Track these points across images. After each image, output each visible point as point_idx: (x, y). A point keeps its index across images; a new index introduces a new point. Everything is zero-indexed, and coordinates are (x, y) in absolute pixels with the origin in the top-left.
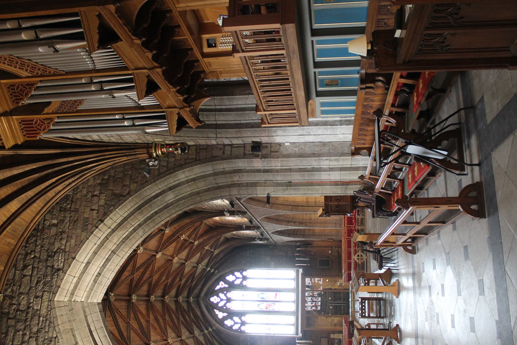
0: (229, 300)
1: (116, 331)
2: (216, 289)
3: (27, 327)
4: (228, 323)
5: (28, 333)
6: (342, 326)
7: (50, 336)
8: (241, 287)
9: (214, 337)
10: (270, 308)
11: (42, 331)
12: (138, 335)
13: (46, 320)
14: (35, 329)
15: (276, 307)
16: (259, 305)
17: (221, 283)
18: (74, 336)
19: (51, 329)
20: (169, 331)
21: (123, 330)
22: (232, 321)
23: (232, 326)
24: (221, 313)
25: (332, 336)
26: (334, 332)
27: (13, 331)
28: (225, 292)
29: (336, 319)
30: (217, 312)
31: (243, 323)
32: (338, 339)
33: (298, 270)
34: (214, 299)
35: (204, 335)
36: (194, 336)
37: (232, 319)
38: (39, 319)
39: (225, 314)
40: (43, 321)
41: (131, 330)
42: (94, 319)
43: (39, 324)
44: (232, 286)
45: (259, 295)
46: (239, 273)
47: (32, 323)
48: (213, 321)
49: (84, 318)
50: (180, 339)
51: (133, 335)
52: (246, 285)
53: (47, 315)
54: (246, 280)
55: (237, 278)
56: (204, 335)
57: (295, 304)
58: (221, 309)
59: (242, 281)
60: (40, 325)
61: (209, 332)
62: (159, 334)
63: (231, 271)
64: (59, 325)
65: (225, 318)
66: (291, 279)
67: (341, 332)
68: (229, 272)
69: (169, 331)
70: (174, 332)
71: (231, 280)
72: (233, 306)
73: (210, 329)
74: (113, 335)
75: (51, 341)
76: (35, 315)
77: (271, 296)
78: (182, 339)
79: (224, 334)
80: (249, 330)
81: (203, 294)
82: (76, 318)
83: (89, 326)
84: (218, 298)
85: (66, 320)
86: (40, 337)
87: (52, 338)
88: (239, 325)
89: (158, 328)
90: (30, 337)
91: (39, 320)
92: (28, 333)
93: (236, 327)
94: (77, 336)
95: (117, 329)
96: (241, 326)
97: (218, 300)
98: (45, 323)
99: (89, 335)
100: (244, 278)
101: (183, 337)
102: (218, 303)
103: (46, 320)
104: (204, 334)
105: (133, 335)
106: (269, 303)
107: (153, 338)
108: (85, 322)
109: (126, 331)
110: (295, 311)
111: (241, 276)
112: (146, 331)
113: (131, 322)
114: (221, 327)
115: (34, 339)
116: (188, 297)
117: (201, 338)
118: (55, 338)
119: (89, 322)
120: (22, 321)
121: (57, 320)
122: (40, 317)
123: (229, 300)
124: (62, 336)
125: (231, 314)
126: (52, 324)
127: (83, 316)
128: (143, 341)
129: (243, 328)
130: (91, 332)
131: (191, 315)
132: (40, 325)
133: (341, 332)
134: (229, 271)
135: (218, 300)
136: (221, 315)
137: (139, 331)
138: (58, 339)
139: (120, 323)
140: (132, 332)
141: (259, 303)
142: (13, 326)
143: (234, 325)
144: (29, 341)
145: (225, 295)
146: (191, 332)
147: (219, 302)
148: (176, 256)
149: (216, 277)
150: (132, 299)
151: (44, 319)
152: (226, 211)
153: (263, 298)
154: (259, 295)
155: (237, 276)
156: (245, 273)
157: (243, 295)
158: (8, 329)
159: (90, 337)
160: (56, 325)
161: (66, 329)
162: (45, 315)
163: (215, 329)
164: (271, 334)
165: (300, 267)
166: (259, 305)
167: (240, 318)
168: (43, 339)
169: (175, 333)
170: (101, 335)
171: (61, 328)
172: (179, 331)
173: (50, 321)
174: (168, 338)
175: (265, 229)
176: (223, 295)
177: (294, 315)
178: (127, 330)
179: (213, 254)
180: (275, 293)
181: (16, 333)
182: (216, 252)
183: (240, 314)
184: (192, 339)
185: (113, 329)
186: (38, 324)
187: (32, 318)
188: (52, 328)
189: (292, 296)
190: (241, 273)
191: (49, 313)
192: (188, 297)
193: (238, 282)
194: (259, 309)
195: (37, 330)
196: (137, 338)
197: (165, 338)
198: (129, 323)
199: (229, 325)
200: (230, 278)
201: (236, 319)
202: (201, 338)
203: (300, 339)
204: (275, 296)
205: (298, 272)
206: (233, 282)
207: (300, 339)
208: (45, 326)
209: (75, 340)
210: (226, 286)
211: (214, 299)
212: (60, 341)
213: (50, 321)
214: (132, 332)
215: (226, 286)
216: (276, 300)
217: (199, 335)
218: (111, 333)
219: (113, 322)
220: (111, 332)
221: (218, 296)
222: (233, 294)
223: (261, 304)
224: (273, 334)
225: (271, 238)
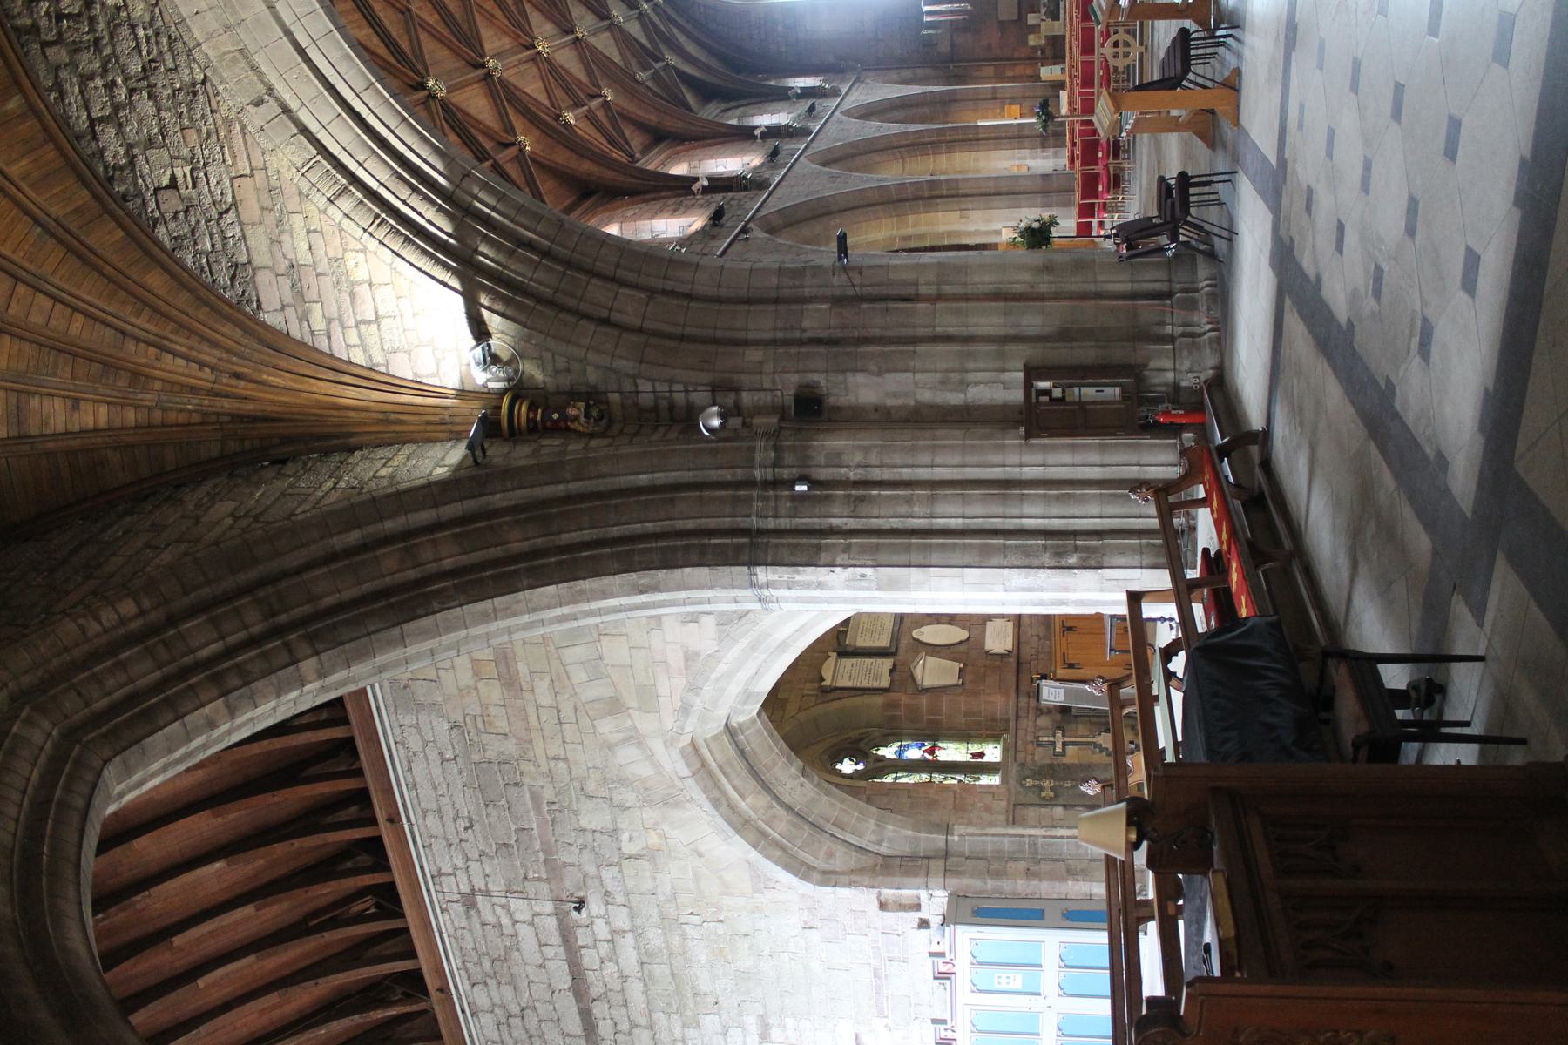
1: (376, 40)
3: (109, 61)
5: (120, 81)
7: (187, 79)
9: (670, 19)
11: (156, 68)
12: (444, 44)
13: (157, 34)
14: (135, 67)
18: (255, 69)
19: (182, 59)
20: (535, 18)
21: (394, 34)
27: (75, 80)
35: (641, 17)
36: (612, 24)
38: (136, 35)
40: (148, 39)
41: (420, 30)
42: (297, 10)
43: (140, 52)
47: (119, 49)
49: (267, 11)
50: (571, 37)
51: (428, 43)
53: (152, 19)
56: (641, 17)
60: (144, 52)
62: (504, 32)
64: (198, 45)
69: (535, 18)
70: (549, 18)
74: (367, 49)
75: (195, 94)
76: (119, 25)
78: (577, 38)
79: (702, 9)
82: (243, 17)
83: (288, 33)
85: (215, 25)
86: (160, 85)
87: (193, 85)
89: (498, 13)
90: (132, 91)
91: (136, 38)
92: (120, 81)
94: (263, 69)
95: (376, 32)
98: (157, 43)
99: (299, 60)
103: (157, 34)
104: (640, 14)
105: (428, 43)
107: (488, 46)
108: (274, 23)
109: (406, 37)
112: (465, 27)
113: (414, 10)
115: (145, 94)
117: (634, 29)
118: (203, 82)
119: (288, 24)
120: (88, 48)
121: (188, 29)
122: (133, 27)
124: (221, 76)
126: (180, 44)
127: (264, 7)
128: (464, 59)
130: (301, 52)
132: (144, 52)
137: (445, 32)
138: (213, 85)
139: (381, 15)
140: (423, 36)
142: (66, 65)
144: (131, 102)
146: (602, 14)
151: (150, 32)
158: (57, 76)
159: (303, 65)
160: (192, 45)
161: (224, 54)
162: (147, 18)
168: (170, 91)
169: (554, 22)
170: (334, 56)
171: (211, 53)
172: (564, 16)
173: (170, 37)
174: (533, 39)
178: (408, 32)
181: (86, 86)
184: (607, 34)
185: (365, 33)
186: (138, 48)
187: (111, 38)
188: (185, 57)
191: (157, 12)
195: (144, 68)
196: (443, 53)
197: (526, 40)
198: (409, 10)
202: (634, 29)
208: (161, 53)
209: (262, 82)
212: (221, 88)
213: (170, 37)
214: (423, 36)
217: (627, 19)
218: (360, 48)
219: (358, 16)
220: (361, 44)
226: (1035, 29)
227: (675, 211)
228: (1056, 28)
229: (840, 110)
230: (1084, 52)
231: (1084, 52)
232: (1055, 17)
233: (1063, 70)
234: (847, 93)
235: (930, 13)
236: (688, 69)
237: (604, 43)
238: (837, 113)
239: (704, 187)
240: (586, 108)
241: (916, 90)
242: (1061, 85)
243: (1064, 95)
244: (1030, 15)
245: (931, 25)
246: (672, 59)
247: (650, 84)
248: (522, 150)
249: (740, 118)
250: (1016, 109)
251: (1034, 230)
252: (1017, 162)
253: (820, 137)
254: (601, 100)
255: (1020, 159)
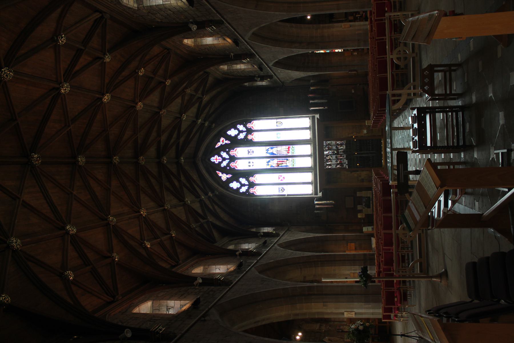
0: (233, 159)
2: (216, 147)
4: (234, 185)
6: (370, 181)
8: (247, 142)
10: (283, 165)
15: (289, 163)
16: (269, 162)
17: (222, 139)
22: (238, 184)
23: (238, 189)
24: (225, 175)
25: (358, 194)
26: (361, 189)
28: (227, 150)
29: (364, 174)
30: (220, 174)
31: (252, 185)
32: (367, 197)
33: (314, 116)
34: (216, 159)
35: (201, 202)
37: (238, 181)
39: (229, 176)
44: (235, 142)
45: (268, 150)
46: (242, 126)
48: (215, 185)
52: (251, 140)
54: (251, 134)
55: (240, 132)
56: (201, 202)
57: (313, 159)
58: (224, 170)
59: (247, 135)
61: (209, 198)
63: (232, 123)
65: (229, 181)
66: (306, 128)
67: (370, 189)
68: (229, 125)
71: (233, 135)
72: (240, 165)
73: (210, 194)
77: (282, 150)
78: (165, 209)
80: (259, 191)
81: (200, 154)
84: (220, 158)
88: (246, 187)
93: (243, 189)
96: (249, 188)
97: (219, 159)
100: (250, 131)
101: (167, 206)
102: (220, 163)
106: (281, 159)
110: (313, 167)
111: (244, 129)
114: (225, 191)
116: (178, 156)
123: (233, 159)
125: (237, 175)
129: (252, 191)
131: (183, 178)
133: (370, 189)
134: (229, 123)
135: (219, 159)
136: (224, 177)
141: (268, 160)
143: (240, 188)
145: (228, 153)
147: (222, 162)
148: (140, 101)
149: (215, 132)
150: (79, 161)
152: (192, 23)
153: (273, 154)
154: (268, 150)
155: (241, 129)
156: (249, 125)
157: (249, 152)
163: (217, 193)
164: (284, 195)
165: (315, 112)
166: (269, 162)
167: (247, 180)
175: (263, 57)
176: (225, 153)
177: (311, 172)
179: (201, 101)
180: (287, 147)
182: (206, 98)
183: (248, 174)
184: (181, 208)
189: (307, 149)
190: (245, 126)
192: (178, 156)
193: (242, 136)
194: (269, 167)
199: (235, 188)
200: (232, 132)
201: (243, 181)
203: (319, 199)
204: (287, 150)
205: (313, 118)
206: (236, 136)
207: (319, 199)
210: (227, 142)
211: (216, 159)
215: (227, 142)
216: (290, 154)
221: (220, 155)
222: (240, 152)
223: (271, 161)
224: (288, 195)
225: (275, 75)
226: (361, 211)
227: (182, 295)
228: (369, 211)
229: (278, 243)
230: (385, 229)
231: (385, 229)
232: (369, 207)
233: (373, 229)
234: (282, 236)
235: (317, 204)
236: (218, 223)
237: (180, 212)
238: (276, 245)
239: (200, 283)
240: (159, 239)
241: (311, 235)
242: (372, 235)
243: (374, 240)
244: (358, 206)
245: (318, 209)
246: (211, 219)
247: (197, 229)
248: (114, 260)
249: (236, 244)
250: (353, 245)
251: (360, 330)
252: (353, 272)
253: (265, 257)
254: (169, 236)
255: (354, 270)
